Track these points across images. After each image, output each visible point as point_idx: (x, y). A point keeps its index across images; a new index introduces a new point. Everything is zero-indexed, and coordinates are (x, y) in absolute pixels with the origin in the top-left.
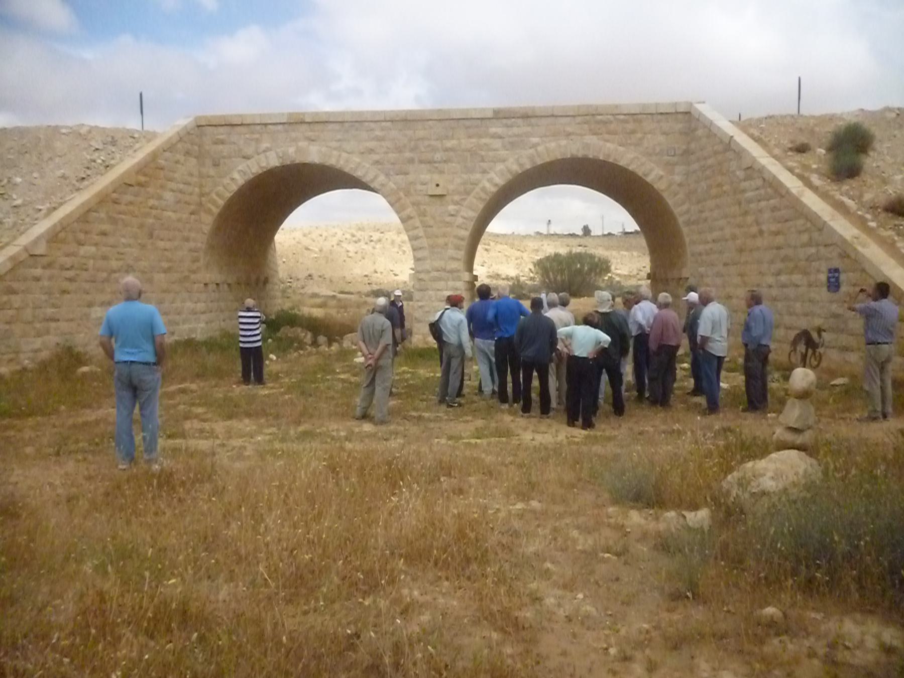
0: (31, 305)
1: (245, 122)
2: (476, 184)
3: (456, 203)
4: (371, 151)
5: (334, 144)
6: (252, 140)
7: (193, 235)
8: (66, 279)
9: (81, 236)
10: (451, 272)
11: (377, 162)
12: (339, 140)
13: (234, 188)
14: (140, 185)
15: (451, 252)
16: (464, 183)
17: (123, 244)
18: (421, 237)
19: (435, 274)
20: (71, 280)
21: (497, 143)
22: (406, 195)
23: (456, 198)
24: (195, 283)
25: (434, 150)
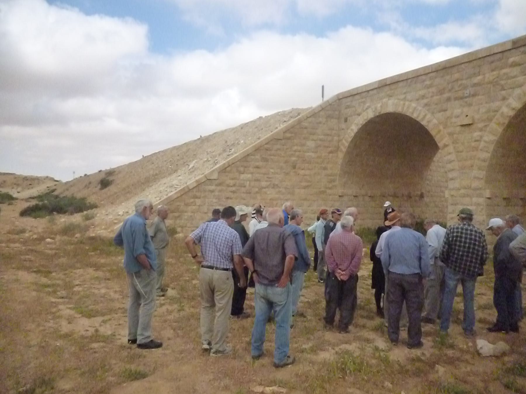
0: (207, 204)
1: (358, 92)
2: (497, 111)
3: (481, 130)
4: (423, 97)
5: (402, 97)
6: (362, 102)
7: (329, 166)
8: (232, 192)
9: (242, 169)
10: (476, 189)
11: (426, 105)
12: (405, 93)
13: (353, 135)
14: (289, 139)
15: (475, 172)
16: (488, 111)
17: (272, 173)
18: (454, 161)
19: (462, 191)
20: (234, 192)
21: (516, 71)
22: (444, 128)
23: (481, 125)
24: (330, 195)
25: (465, 88)
